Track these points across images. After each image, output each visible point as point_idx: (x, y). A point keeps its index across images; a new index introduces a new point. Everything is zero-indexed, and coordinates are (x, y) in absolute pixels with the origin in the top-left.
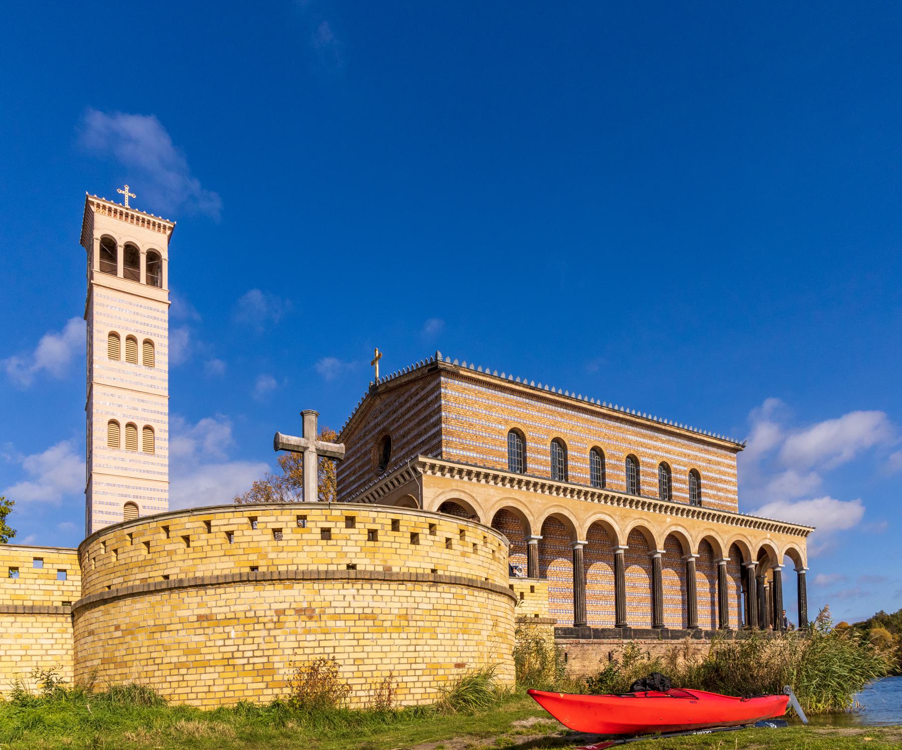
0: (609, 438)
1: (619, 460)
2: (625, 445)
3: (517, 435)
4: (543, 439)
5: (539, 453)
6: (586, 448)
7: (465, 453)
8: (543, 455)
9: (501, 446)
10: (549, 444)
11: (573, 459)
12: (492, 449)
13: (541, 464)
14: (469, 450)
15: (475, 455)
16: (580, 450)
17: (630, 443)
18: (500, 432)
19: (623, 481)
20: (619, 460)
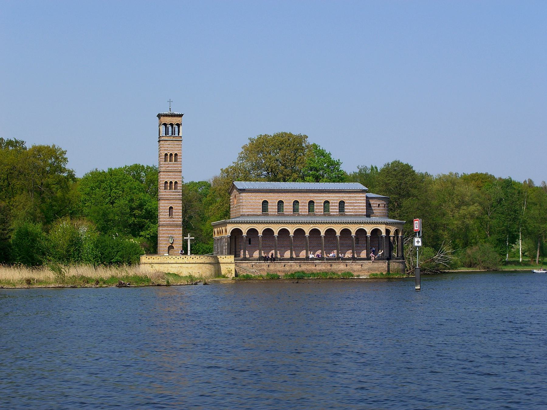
0: (301, 197)
1: (305, 203)
2: (308, 198)
3: (265, 203)
4: (275, 202)
5: (273, 206)
6: (291, 202)
7: (247, 210)
8: (275, 206)
9: (259, 206)
10: (277, 203)
11: (286, 206)
12: (257, 208)
13: (274, 209)
14: (249, 209)
15: (251, 210)
16: (289, 203)
17: (310, 197)
18: (259, 203)
19: (307, 209)
20: (305, 203)
